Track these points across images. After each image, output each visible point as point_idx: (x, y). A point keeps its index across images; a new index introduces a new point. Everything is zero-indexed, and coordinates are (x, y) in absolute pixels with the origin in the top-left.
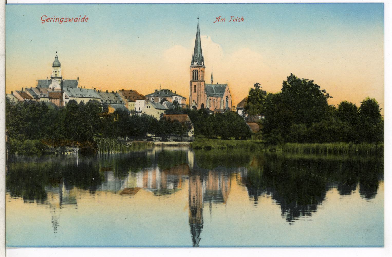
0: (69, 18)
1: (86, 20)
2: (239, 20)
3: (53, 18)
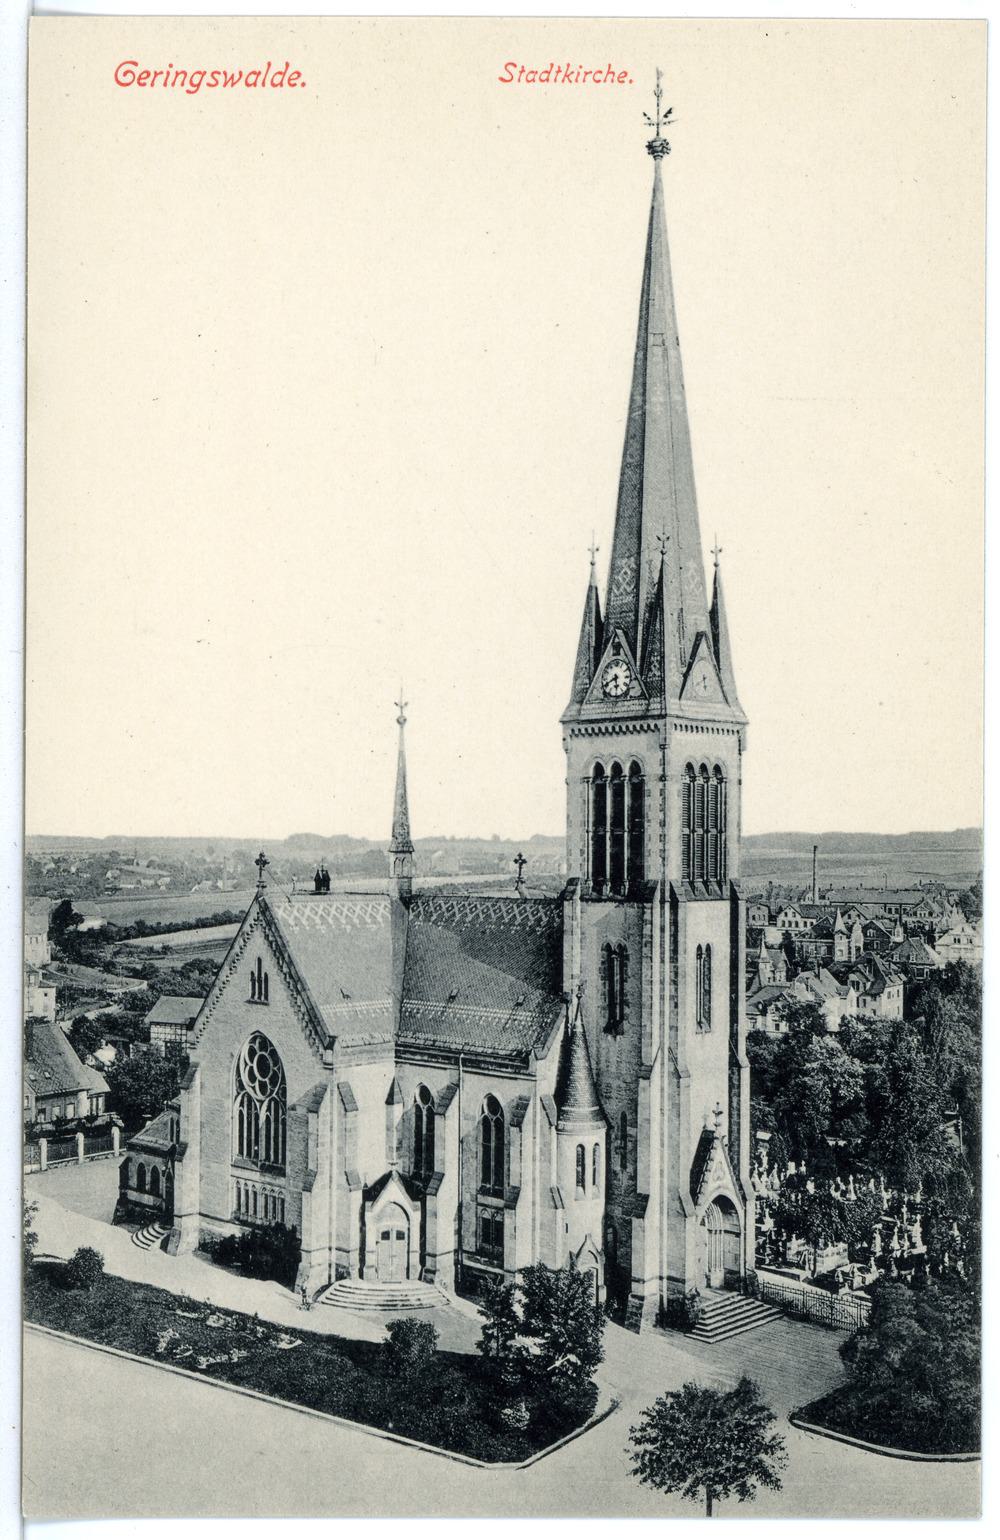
0: (225, 74)
1: (289, 79)
2: (598, 77)
3: (161, 73)
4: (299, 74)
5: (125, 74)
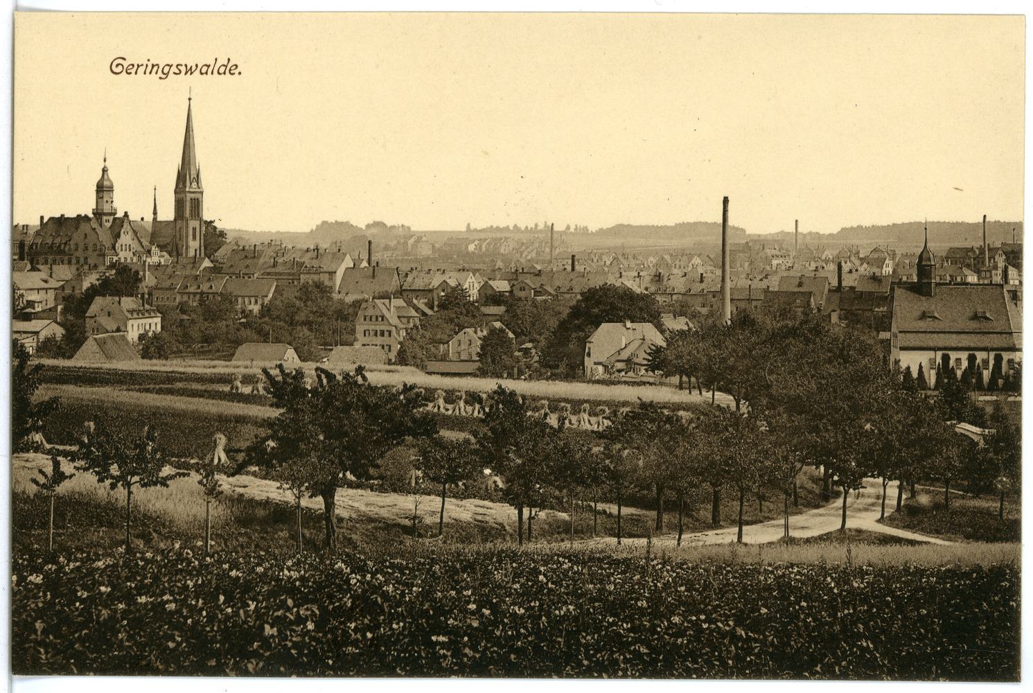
0: (186, 66)
1: (230, 70)
3: (142, 65)
4: (236, 66)
5: (117, 65)
